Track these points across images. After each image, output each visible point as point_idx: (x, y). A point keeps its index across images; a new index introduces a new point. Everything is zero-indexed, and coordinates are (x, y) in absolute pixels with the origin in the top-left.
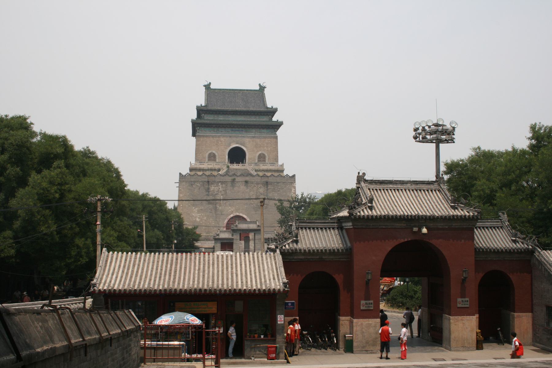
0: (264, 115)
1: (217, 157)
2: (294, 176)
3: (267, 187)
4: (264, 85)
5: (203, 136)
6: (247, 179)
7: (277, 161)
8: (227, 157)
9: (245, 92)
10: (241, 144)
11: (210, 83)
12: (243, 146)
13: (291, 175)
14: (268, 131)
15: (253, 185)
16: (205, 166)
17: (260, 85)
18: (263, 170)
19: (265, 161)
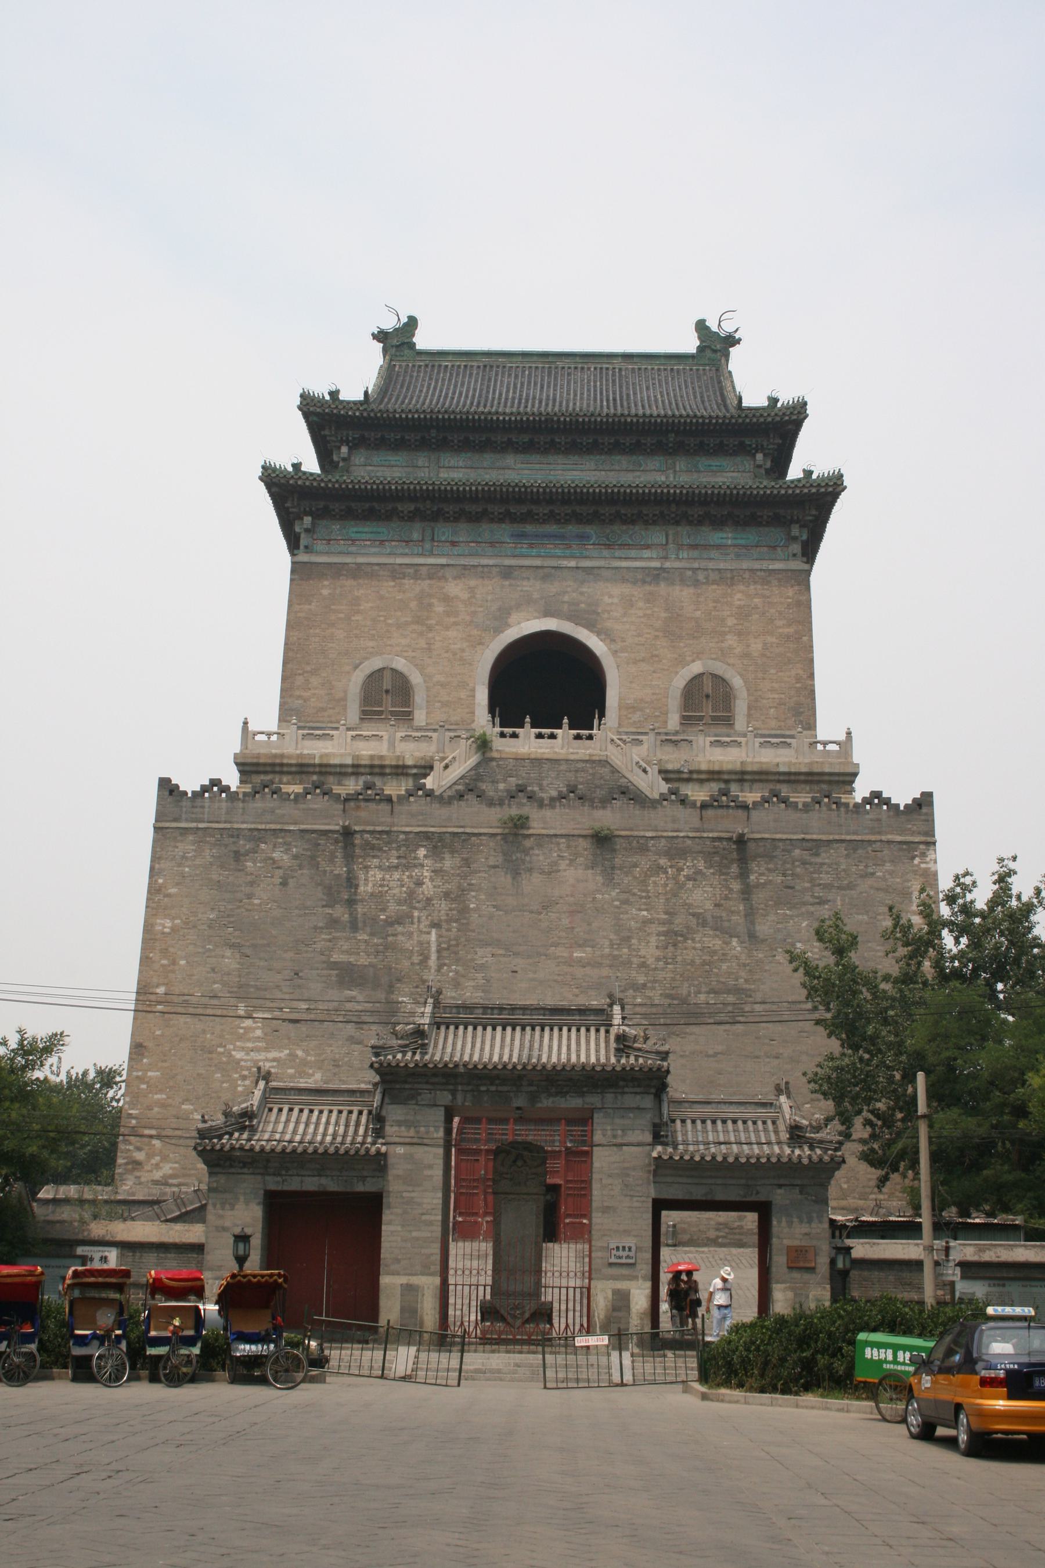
0: (720, 450)
1: (419, 697)
2: (924, 803)
3: (744, 875)
4: (728, 327)
5: (337, 571)
6: (608, 818)
7: (810, 725)
8: (482, 696)
9: (617, 363)
10: (574, 617)
11: (412, 323)
12: (590, 626)
13: (902, 798)
14: (750, 536)
15: (645, 862)
16: (336, 748)
17: (701, 326)
18: (714, 775)
19: (726, 720)
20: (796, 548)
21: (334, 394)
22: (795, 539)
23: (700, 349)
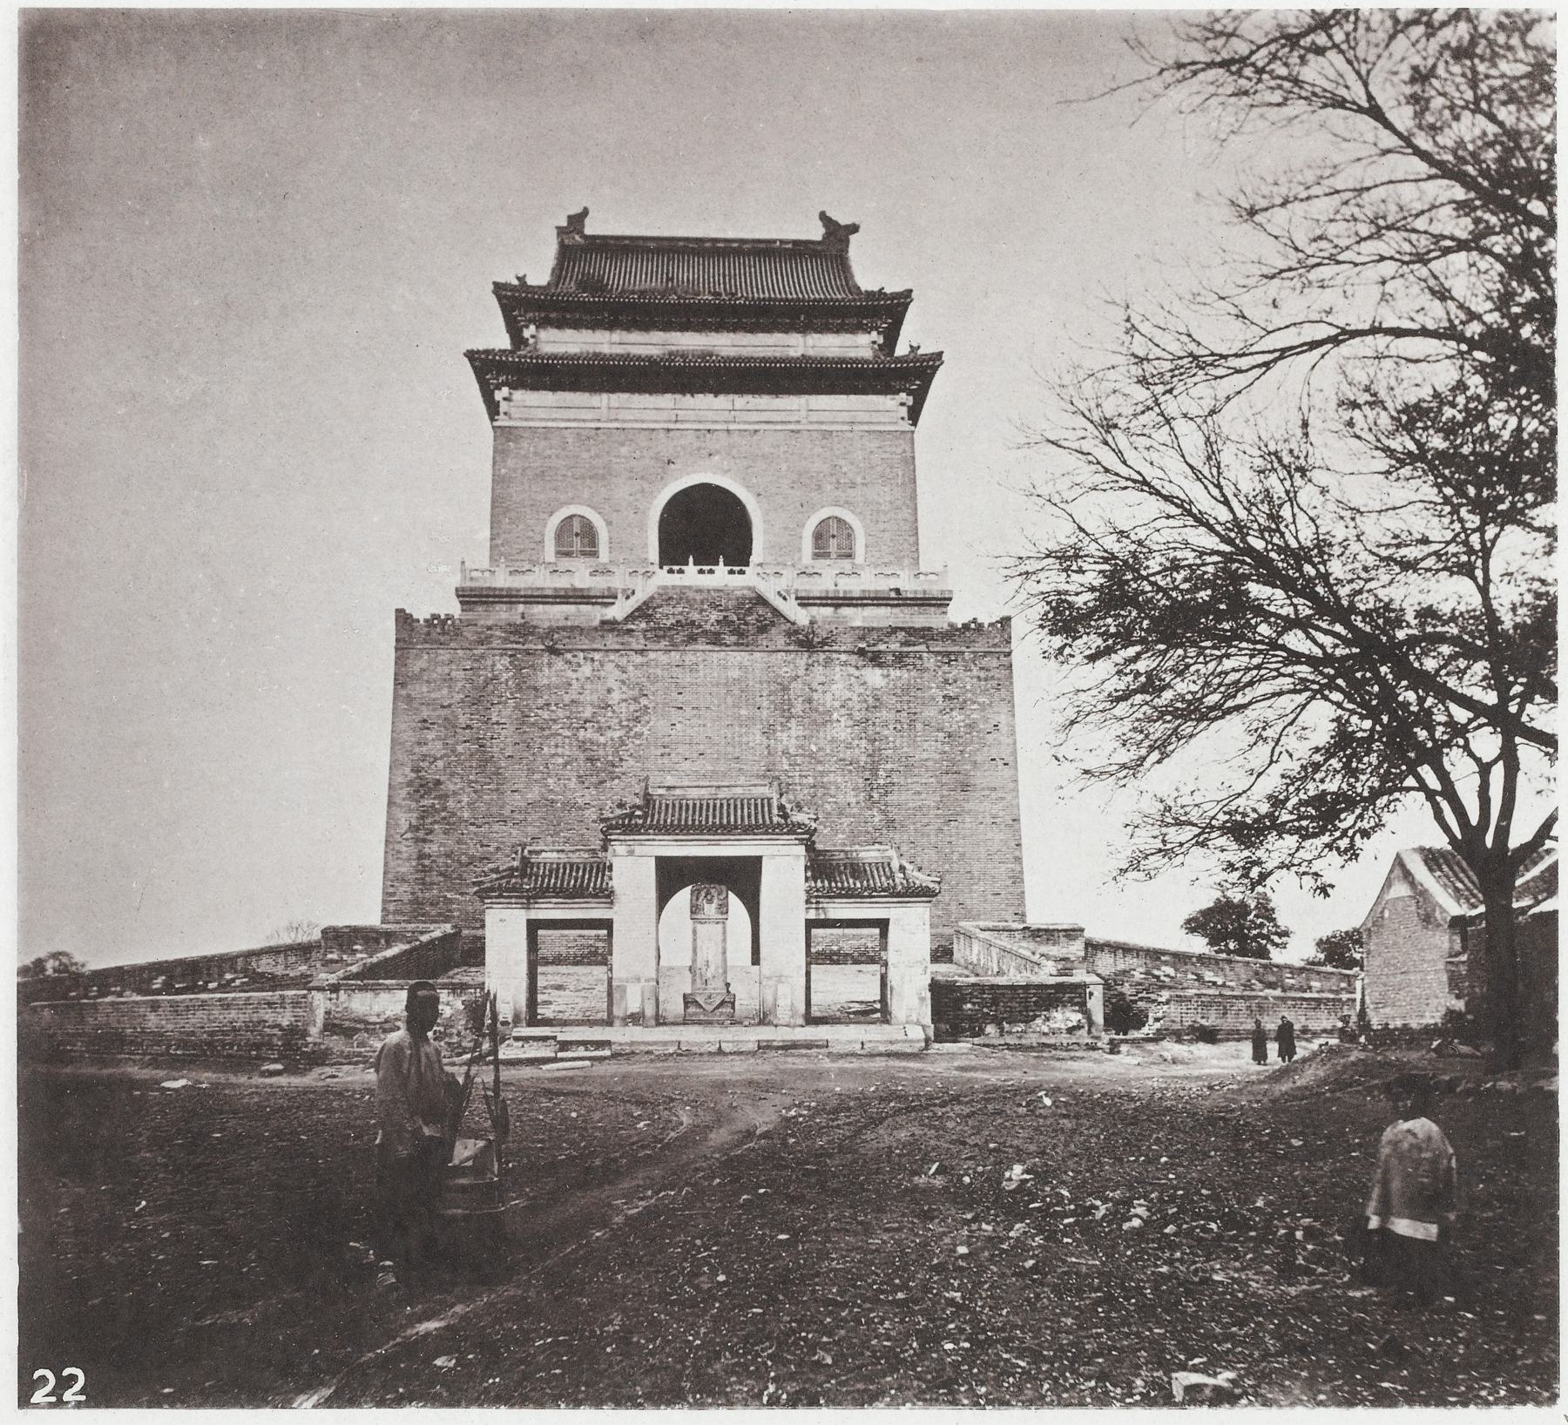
20: (904, 411)
21: (521, 279)
22: (902, 404)
23: (827, 236)
